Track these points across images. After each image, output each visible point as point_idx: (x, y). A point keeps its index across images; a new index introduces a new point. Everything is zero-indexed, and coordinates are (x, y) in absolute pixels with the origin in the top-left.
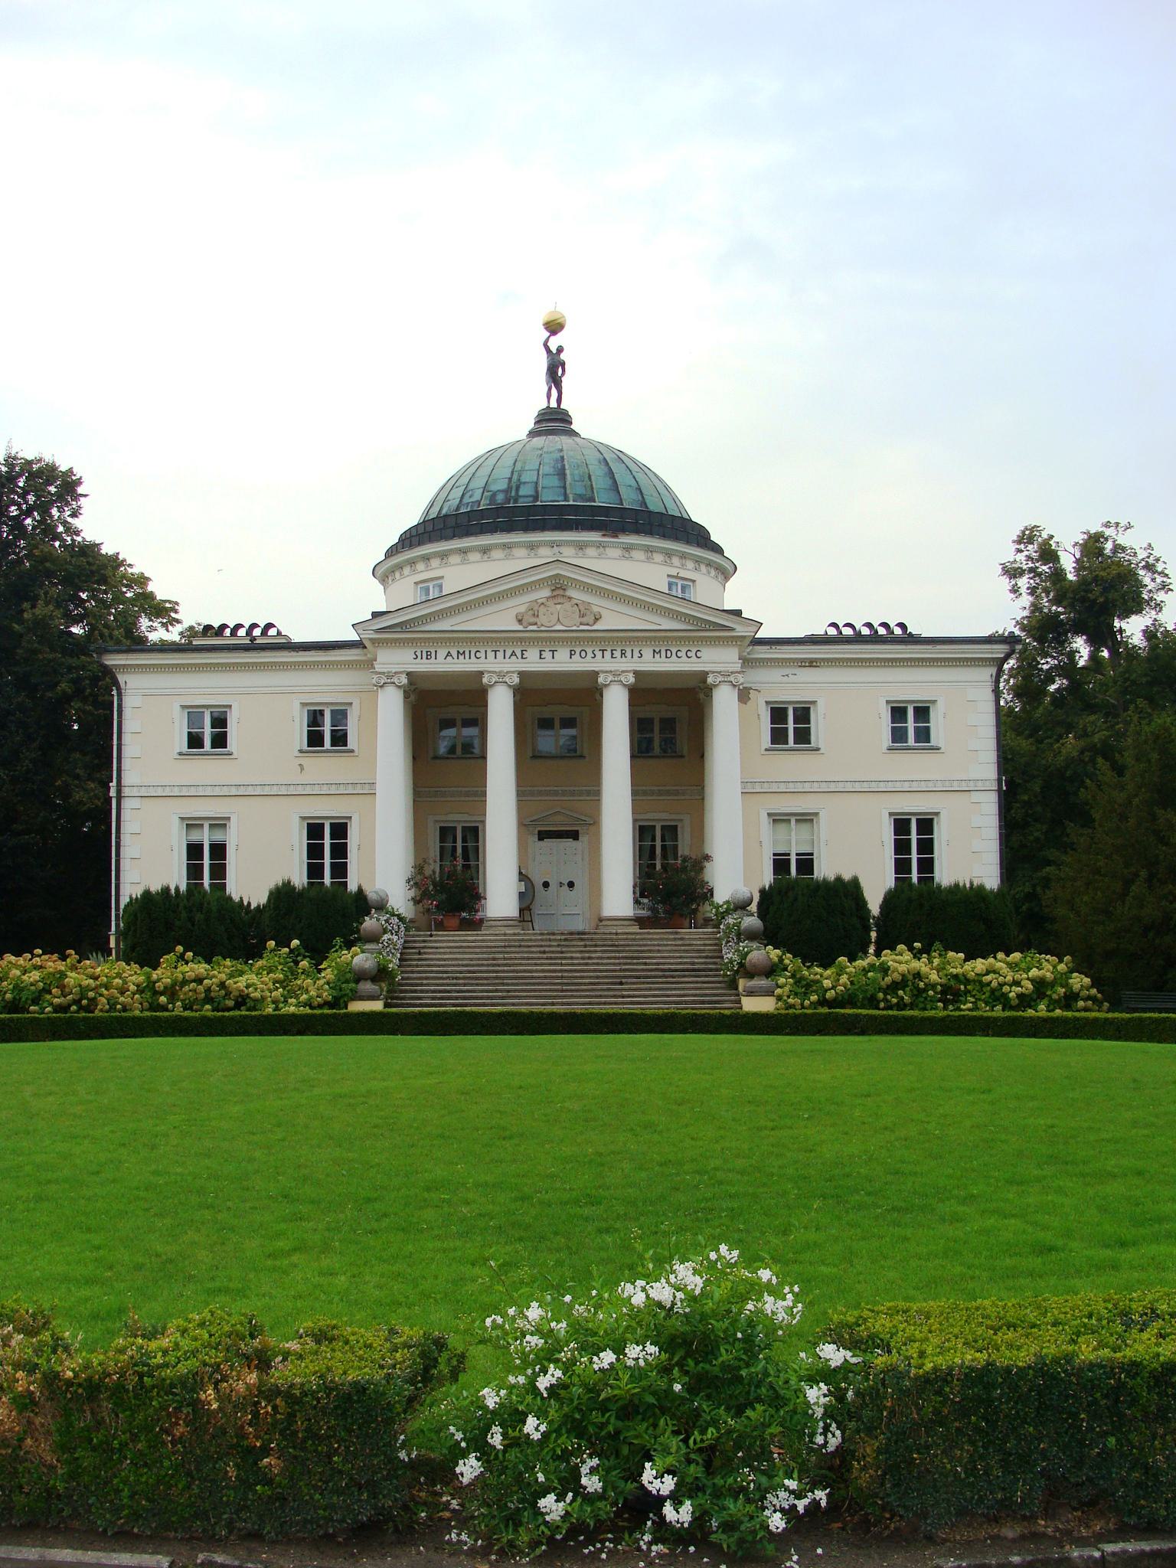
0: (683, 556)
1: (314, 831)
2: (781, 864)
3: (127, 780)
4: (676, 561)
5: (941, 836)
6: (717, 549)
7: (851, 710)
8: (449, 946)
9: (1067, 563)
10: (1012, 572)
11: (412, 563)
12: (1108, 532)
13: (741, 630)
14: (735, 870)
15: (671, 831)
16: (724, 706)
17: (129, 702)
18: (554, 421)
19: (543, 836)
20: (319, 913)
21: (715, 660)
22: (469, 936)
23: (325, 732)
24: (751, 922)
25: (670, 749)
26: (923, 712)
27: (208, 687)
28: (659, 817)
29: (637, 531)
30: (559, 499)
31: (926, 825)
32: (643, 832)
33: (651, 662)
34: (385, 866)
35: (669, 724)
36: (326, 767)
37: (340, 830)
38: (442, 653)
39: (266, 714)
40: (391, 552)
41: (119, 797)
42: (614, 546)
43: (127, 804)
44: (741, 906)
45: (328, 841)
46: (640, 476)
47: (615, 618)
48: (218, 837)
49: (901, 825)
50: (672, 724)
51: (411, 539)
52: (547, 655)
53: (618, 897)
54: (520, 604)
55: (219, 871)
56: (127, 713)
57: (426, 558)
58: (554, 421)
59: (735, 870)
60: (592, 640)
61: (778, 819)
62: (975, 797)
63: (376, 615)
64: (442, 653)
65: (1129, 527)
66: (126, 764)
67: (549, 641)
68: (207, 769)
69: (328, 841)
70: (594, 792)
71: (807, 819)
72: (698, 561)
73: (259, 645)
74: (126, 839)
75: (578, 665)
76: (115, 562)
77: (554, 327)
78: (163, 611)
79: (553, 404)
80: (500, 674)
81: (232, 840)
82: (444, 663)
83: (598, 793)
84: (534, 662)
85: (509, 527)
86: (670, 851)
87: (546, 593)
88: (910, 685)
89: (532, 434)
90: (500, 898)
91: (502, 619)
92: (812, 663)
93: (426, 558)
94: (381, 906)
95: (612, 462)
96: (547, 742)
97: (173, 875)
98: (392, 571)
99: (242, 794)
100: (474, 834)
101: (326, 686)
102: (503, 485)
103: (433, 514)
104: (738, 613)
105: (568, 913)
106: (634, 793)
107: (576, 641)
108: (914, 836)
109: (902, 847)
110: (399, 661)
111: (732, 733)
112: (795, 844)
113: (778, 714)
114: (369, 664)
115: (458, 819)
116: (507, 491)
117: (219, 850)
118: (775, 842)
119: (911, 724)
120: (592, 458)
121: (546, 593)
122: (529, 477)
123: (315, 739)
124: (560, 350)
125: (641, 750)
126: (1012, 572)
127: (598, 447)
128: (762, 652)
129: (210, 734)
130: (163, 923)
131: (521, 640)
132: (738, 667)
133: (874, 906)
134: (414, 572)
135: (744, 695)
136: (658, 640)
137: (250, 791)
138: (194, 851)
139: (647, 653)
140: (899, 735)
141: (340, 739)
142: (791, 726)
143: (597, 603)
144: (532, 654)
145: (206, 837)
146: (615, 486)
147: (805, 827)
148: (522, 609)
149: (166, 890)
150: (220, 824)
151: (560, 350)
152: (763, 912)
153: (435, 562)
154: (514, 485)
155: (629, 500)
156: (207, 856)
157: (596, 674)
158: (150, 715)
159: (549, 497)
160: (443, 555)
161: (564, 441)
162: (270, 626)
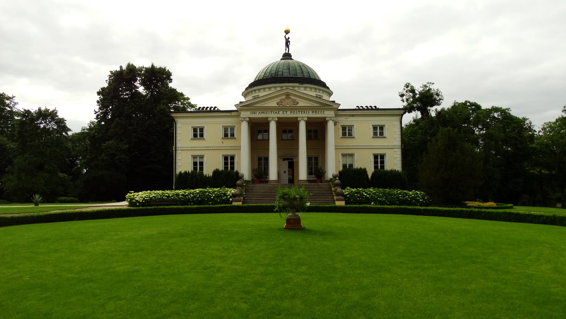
0: (320, 90)
1: (226, 158)
2: (344, 166)
3: (179, 145)
4: (318, 91)
5: (387, 159)
6: (328, 88)
7: (363, 128)
8: (259, 187)
9: (417, 92)
10: (402, 96)
11: (251, 92)
12: (428, 85)
13: (335, 106)
14: (332, 168)
15: (316, 159)
16: (331, 126)
17: (178, 125)
18: (287, 56)
19: (284, 160)
21: (329, 114)
22: (265, 185)
23: (229, 133)
24: (338, 181)
25: (316, 138)
26: (382, 128)
27: (198, 122)
29: (308, 83)
30: (288, 76)
31: (382, 157)
32: (309, 159)
33: (312, 115)
34: (244, 167)
35: (316, 131)
36: (229, 143)
37: (232, 158)
38: (258, 113)
39: (213, 129)
40: (247, 89)
41: (176, 150)
42: (302, 87)
43: (178, 152)
44: (335, 177)
45: (229, 160)
46: (309, 70)
47: (302, 103)
48: (201, 160)
49: (376, 157)
50: (317, 131)
52: (285, 113)
54: (278, 100)
55: (202, 169)
56: (178, 129)
57: (255, 91)
58: (287, 56)
59: (332, 168)
60: (296, 109)
61: (344, 155)
62: (395, 150)
63: (240, 102)
64: (258, 113)
65: (433, 84)
66: (178, 142)
67: (285, 109)
68: (198, 143)
69: (229, 160)
70: (297, 148)
71: (352, 155)
72: (323, 91)
73: (212, 112)
74: (177, 161)
75: (293, 115)
76: (182, 94)
77: (287, 32)
79: (287, 52)
80: (273, 118)
81: (205, 161)
82: (258, 115)
83: (298, 149)
84: (281, 115)
85: (275, 83)
86: (317, 164)
87: (284, 97)
88: (378, 121)
89: (282, 59)
90: (273, 175)
91: (273, 103)
92: (353, 115)
93: (255, 91)
94: (242, 177)
95: (302, 67)
96: (285, 136)
98: (247, 94)
99: (207, 149)
100: (267, 159)
101: (229, 122)
102: (274, 72)
103: (257, 79)
104: (334, 102)
106: (307, 149)
108: (379, 159)
109: (376, 162)
110: (246, 114)
111: (332, 133)
112: (348, 161)
113: (344, 128)
114: (239, 116)
115: (263, 155)
116: (276, 73)
117: (201, 164)
118: (343, 161)
119: (378, 131)
120: (297, 65)
121: (284, 97)
122: (280, 70)
123: (226, 135)
124: (289, 38)
125: (309, 138)
126: (402, 96)
127: (298, 63)
128: (340, 113)
129: (198, 133)
131: (278, 109)
132: (334, 116)
133: (370, 176)
134: (252, 94)
135: (335, 124)
136: (313, 109)
137: (209, 148)
138: (195, 164)
139: (311, 112)
140: (375, 134)
141: (232, 135)
142: (347, 132)
143: (298, 99)
144: (281, 113)
145: (198, 160)
146: (303, 72)
147: (351, 157)
148: (278, 101)
149: (186, 172)
150: (202, 157)
151: (289, 38)
152: (340, 179)
153: (257, 91)
154: (277, 71)
155: (306, 75)
156: (198, 164)
157: (297, 118)
158: (183, 129)
159: (286, 75)
160: (259, 90)
161: (290, 61)
162: (215, 107)
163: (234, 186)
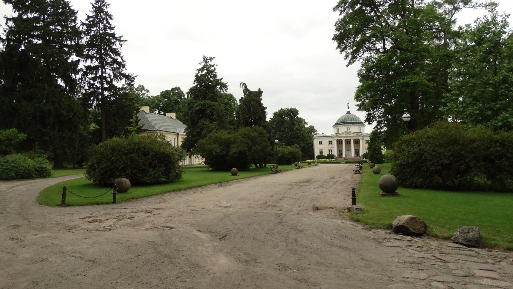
8: (340, 159)
14: (361, 154)
18: (348, 112)
20: (330, 156)
21: (360, 138)
23: (330, 143)
28: (357, 149)
34: (335, 153)
36: (330, 146)
39: (325, 142)
45: (331, 151)
47: (352, 135)
50: (357, 142)
51: (336, 124)
53: (353, 154)
58: (348, 112)
59: (361, 154)
68: (321, 146)
69: (331, 151)
78: (307, 123)
84: (346, 138)
90: (344, 155)
91: (343, 135)
101: (330, 139)
105: (348, 156)
107: (349, 137)
110: (336, 138)
129: (321, 143)
130: (319, 157)
156: (321, 152)
158: (316, 142)
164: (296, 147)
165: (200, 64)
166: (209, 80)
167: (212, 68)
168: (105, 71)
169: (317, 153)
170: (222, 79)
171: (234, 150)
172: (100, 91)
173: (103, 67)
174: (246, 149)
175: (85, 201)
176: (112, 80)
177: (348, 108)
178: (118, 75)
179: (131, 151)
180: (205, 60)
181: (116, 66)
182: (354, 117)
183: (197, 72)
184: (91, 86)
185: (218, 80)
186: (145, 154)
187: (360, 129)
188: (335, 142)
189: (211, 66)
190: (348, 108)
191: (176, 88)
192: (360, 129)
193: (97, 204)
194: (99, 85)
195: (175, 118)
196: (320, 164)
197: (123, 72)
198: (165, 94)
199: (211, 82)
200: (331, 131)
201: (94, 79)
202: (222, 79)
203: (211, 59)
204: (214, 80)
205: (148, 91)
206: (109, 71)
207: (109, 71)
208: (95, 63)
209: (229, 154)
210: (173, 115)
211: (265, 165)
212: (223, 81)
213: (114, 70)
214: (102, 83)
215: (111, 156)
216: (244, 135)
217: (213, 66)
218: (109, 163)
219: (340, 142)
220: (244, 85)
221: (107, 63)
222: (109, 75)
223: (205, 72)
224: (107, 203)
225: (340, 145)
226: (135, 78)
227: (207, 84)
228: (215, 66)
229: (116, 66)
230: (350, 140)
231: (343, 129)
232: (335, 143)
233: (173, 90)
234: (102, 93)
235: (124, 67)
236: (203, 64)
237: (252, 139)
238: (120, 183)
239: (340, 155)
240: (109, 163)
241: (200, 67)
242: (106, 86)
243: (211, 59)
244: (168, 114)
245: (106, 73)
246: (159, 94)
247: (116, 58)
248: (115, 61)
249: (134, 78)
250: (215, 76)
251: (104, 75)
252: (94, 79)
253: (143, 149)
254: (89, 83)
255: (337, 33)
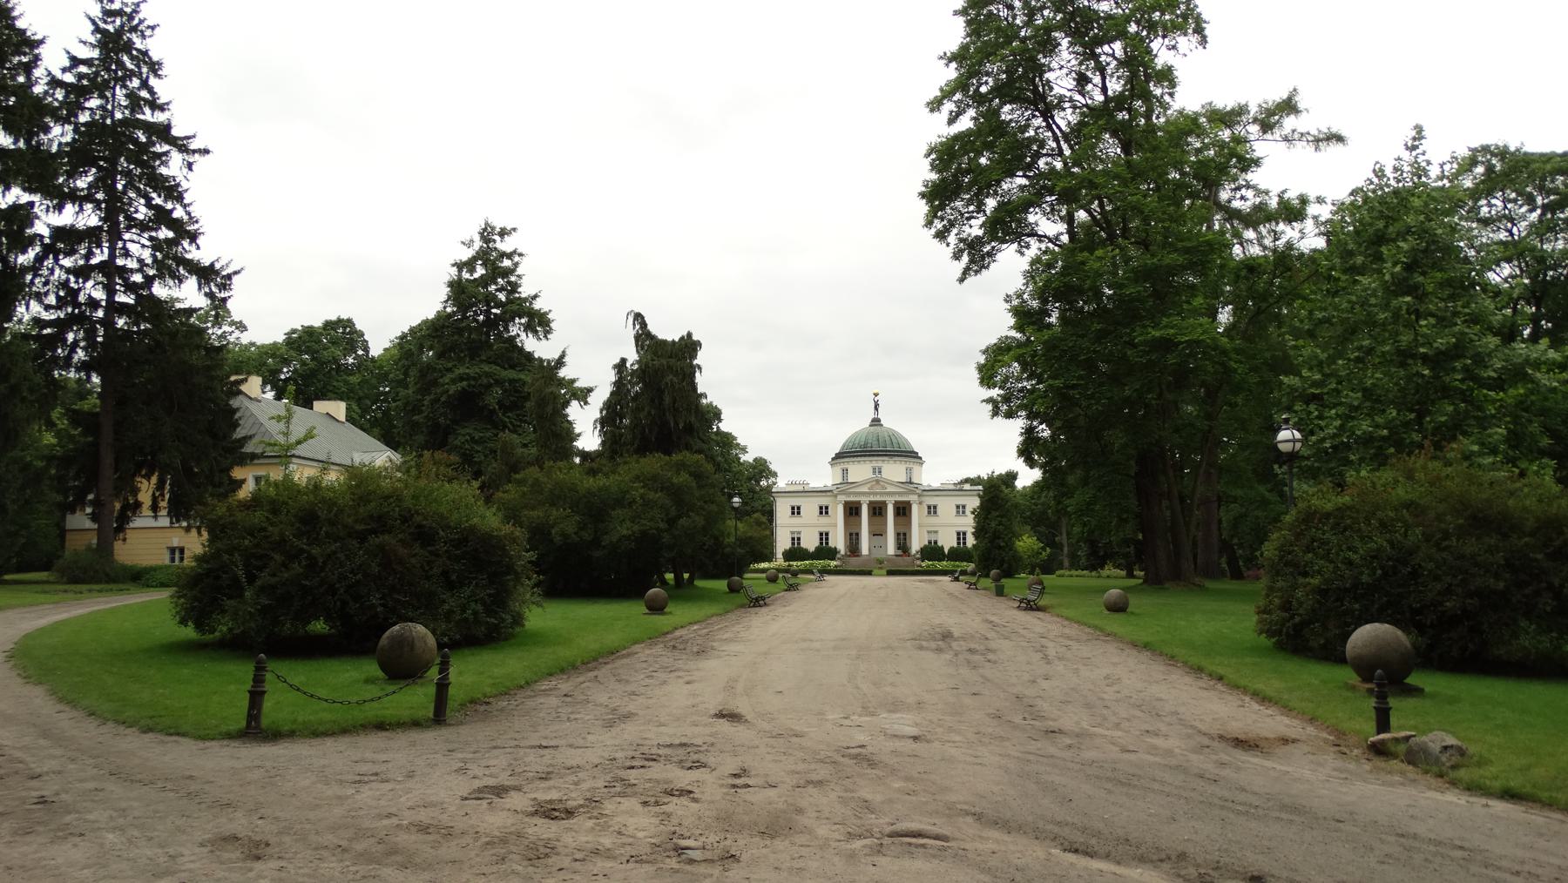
7: (946, 506)
8: (854, 560)
14: (916, 545)
16: (915, 508)
18: (876, 422)
21: (912, 498)
23: (824, 510)
30: (877, 446)
34: (838, 541)
36: (824, 520)
39: (810, 507)
45: (824, 536)
47: (890, 489)
50: (903, 510)
51: (839, 456)
53: (891, 549)
58: (876, 422)
59: (916, 545)
67: (875, 494)
68: (796, 520)
69: (824, 536)
78: (744, 450)
84: (872, 498)
88: (961, 501)
90: (865, 549)
91: (865, 489)
97: (788, 545)
101: (824, 501)
105: (878, 554)
107: (881, 494)
110: (843, 498)
129: (796, 511)
130: (791, 555)
142: (932, 510)
154: (865, 445)
156: (796, 540)
158: (782, 509)
163: (833, 559)
164: (759, 523)
165: (469, 244)
166: (490, 300)
167: (507, 263)
168: (124, 248)
169: (782, 543)
170: (535, 297)
171: (622, 528)
172: (100, 313)
173: (115, 235)
174: (662, 525)
175: (326, 715)
176: (149, 281)
177: (876, 408)
178: (171, 263)
179: (380, 523)
180: (487, 234)
181: (165, 233)
182: (893, 436)
183: (454, 271)
184: (69, 296)
185: (525, 300)
186: (424, 536)
187: (909, 470)
188: (840, 509)
189: (503, 255)
190: (876, 408)
191: (340, 321)
192: (909, 470)
193: (381, 726)
194: (99, 294)
195: (342, 417)
196: (827, 578)
197: (188, 256)
198: (304, 340)
199: (499, 304)
200: (824, 477)
201: (83, 272)
202: (535, 297)
203: (503, 233)
204: (510, 301)
205: (241, 327)
206: (138, 248)
207: (138, 248)
208: (90, 218)
209: (606, 541)
210: (339, 409)
211: (691, 580)
212: (537, 305)
213: (156, 245)
214: (110, 291)
215: (302, 544)
216: (651, 481)
217: (510, 256)
218: (297, 568)
219: (852, 510)
220: (639, 318)
221: (132, 223)
222: (140, 261)
223: (480, 271)
224: (416, 724)
225: (852, 519)
226: (235, 279)
227: (484, 313)
228: (517, 259)
229: (165, 233)
230: (884, 504)
231: (860, 471)
232: (839, 513)
233: (329, 325)
234: (108, 323)
235: (193, 237)
236: (478, 244)
237: (676, 493)
238: (404, 642)
239: (854, 548)
240: (297, 568)
241: (466, 254)
242: (122, 298)
243: (503, 233)
244: (320, 406)
245: (127, 254)
246: (280, 338)
247: (169, 206)
248: (162, 217)
249: (229, 277)
250: (514, 287)
251: (120, 262)
252: (83, 272)
253: (418, 519)
254: (65, 285)
255: (934, 176)
